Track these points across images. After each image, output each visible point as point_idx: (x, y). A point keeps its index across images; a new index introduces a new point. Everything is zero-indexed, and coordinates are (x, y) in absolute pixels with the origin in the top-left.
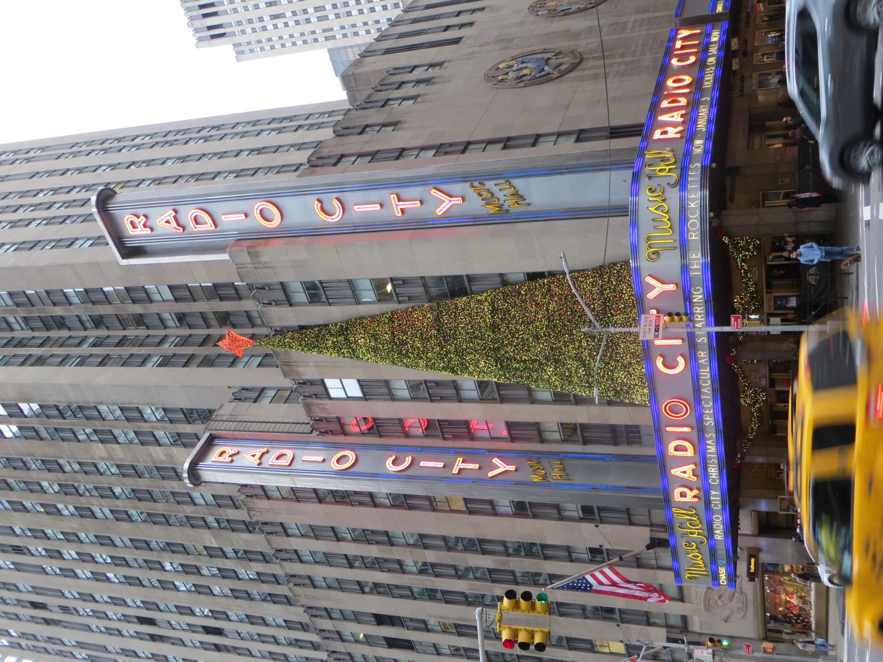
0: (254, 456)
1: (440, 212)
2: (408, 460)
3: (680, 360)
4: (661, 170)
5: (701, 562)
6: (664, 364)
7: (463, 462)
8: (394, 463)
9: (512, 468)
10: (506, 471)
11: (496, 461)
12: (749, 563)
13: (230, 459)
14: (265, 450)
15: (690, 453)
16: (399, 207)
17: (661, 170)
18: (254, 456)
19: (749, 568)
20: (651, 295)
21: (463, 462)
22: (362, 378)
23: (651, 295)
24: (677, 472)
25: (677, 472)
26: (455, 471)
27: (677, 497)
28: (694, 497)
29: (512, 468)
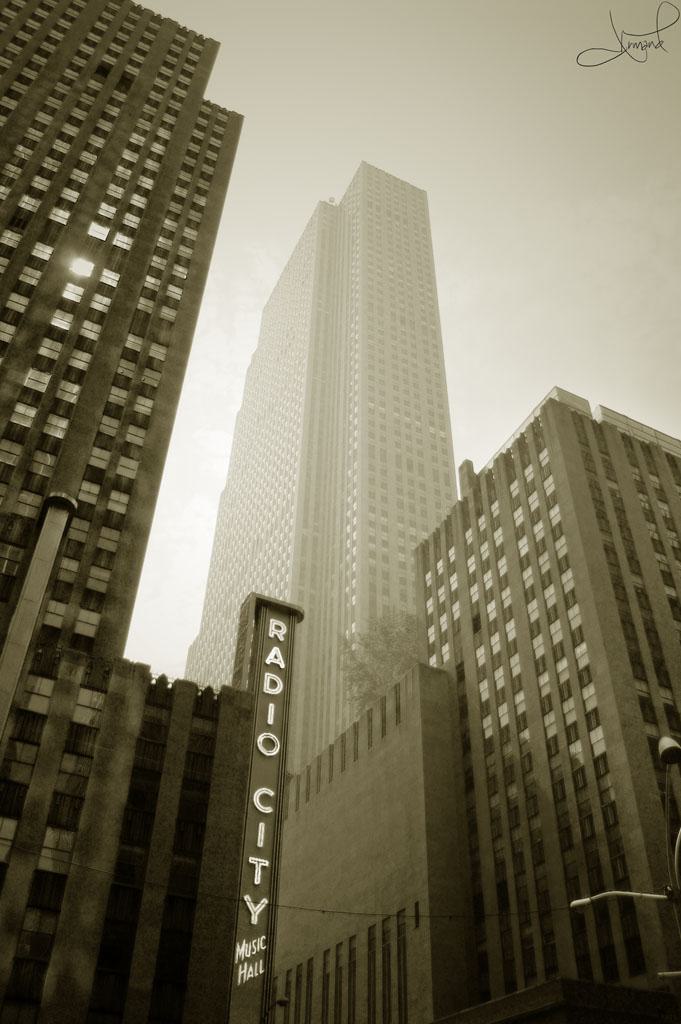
2: (268, 810)
7: (263, 868)
8: (264, 799)
9: (255, 920)
13: (271, 635)
14: (283, 666)
18: (276, 657)
21: (263, 868)
26: (252, 860)
29: (255, 920)
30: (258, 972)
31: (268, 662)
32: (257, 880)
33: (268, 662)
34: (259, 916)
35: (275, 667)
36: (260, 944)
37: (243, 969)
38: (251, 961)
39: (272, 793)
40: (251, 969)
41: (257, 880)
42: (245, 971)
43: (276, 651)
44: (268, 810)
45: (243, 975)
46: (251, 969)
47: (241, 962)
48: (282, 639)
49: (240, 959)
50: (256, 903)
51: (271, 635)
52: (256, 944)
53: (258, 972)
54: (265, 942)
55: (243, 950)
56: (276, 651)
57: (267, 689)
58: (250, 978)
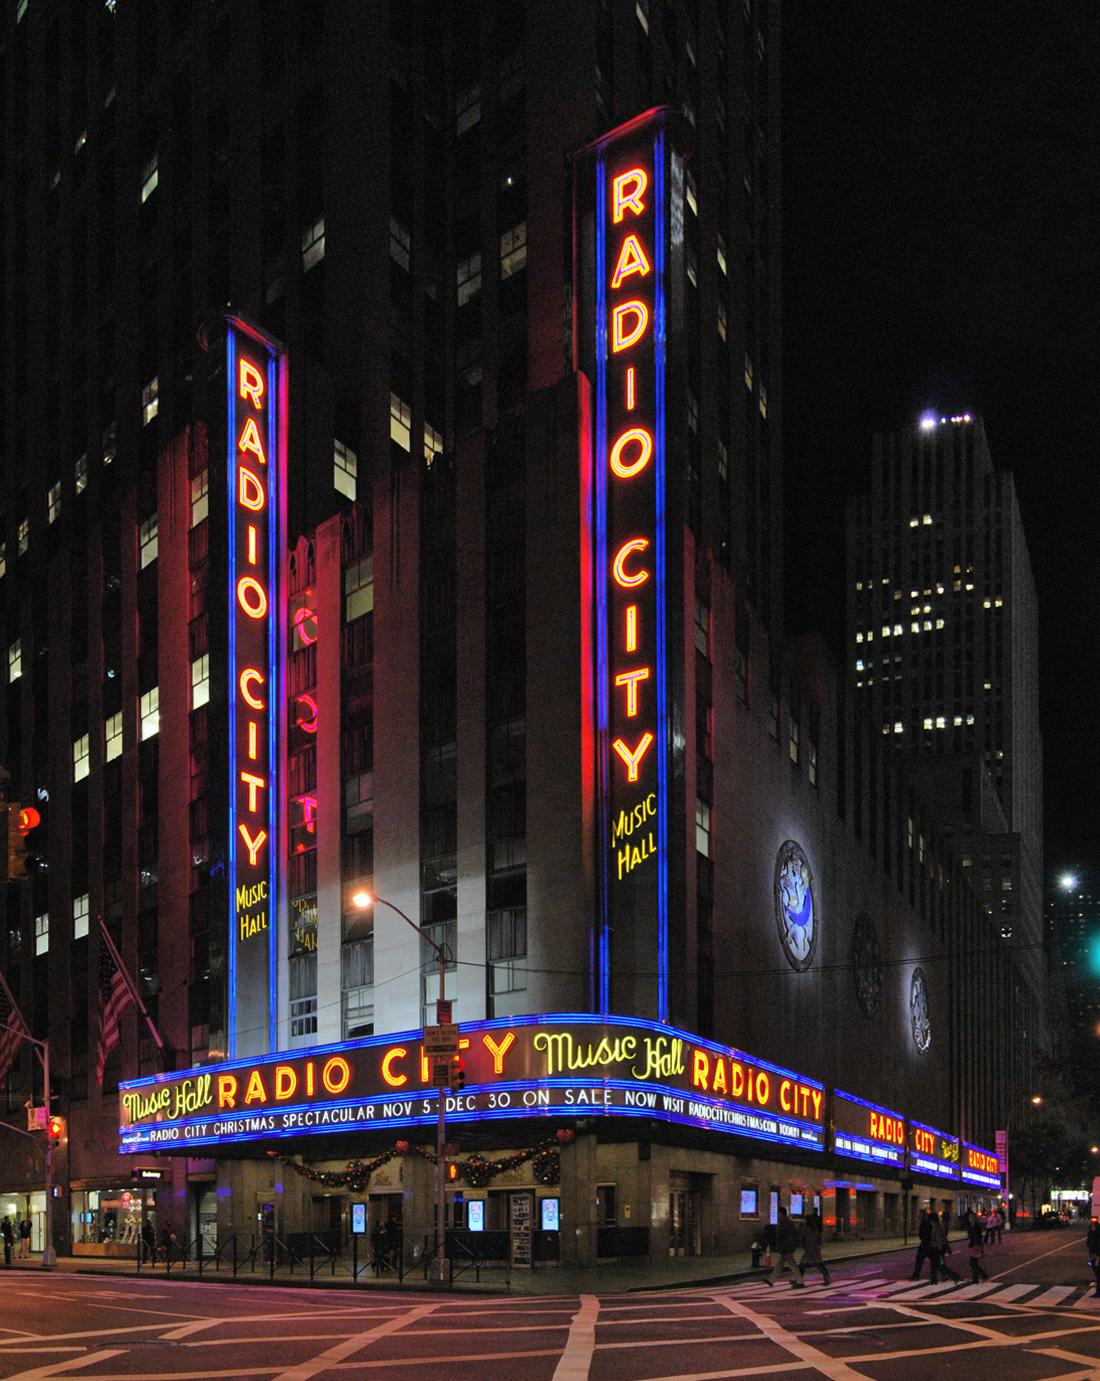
1: (620, 747)
5: (147, 1112)
9: (253, 860)
16: (629, 682)
22: (376, 621)
27: (222, 1081)
29: (253, 860)
30: (261, 927)
36: (259, 893)
37: (245, 922)
38: (252, 912)
40: (253, 921)
42: (247, 924)
45: (245, 928)
46: (253, 921)
47: (244, 912)
49: (241, 907)
52: (256, 890)
53: (261, 927)
54: (266, 890)
55: (242, 898)
58: (253, 933)
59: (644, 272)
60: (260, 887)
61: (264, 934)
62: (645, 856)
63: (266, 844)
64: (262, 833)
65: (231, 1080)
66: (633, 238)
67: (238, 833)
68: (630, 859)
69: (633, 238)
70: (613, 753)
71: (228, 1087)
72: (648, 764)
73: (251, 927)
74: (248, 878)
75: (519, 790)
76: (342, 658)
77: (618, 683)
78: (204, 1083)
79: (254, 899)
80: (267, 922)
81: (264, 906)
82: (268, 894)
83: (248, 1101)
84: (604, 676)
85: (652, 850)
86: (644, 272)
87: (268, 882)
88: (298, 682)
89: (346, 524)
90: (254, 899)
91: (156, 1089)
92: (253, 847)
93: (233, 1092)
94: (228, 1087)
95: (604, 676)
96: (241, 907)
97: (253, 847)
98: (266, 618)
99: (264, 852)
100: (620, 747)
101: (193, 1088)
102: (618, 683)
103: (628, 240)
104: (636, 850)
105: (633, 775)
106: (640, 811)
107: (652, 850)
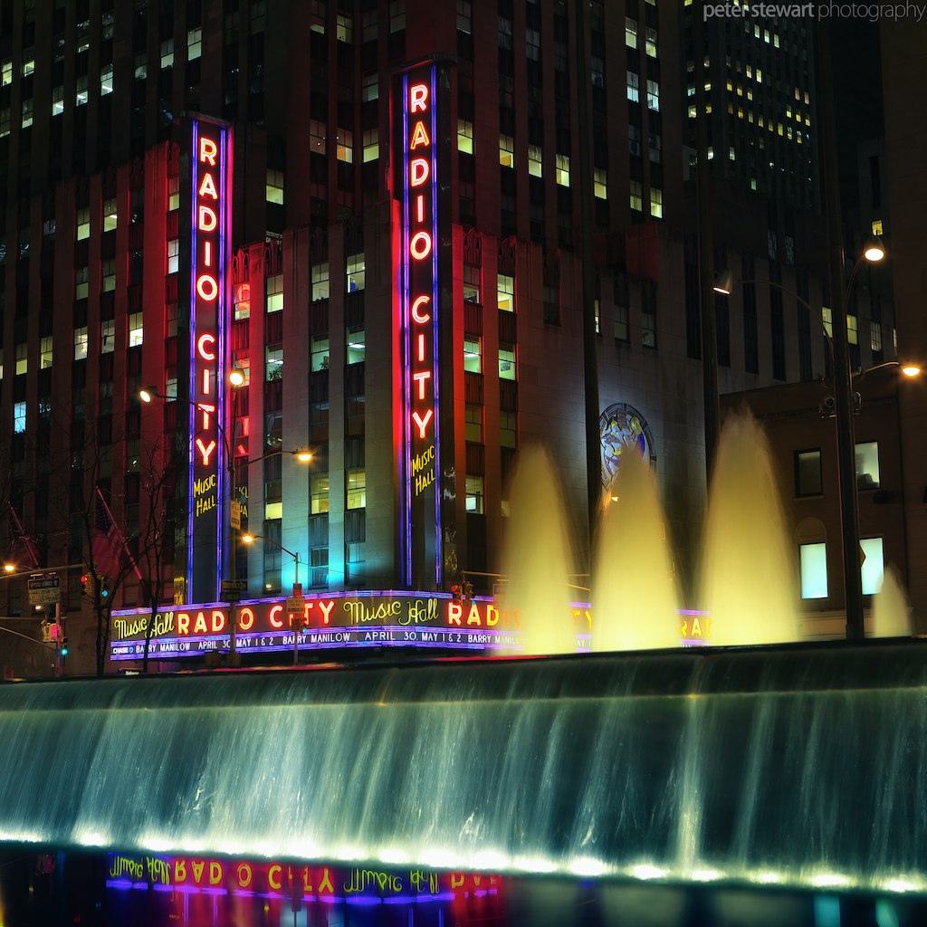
0: (208, 186)
3: (279, 624)
4: (414, 613)
5: (131, 633)
6: (277, 612)
9: (206, 461)
10: (202, 457)
11: (212, 445)
12: (133, 671)
13: (203, 159)
14: (215, 197)
15: (215, 628)
17: (414, 613)
18: (208, 186)
19: (129, 671)
20: (321, 605)
21: (209, 413)
23: (321, 605)
24: (201, 617)
25: (201, 617)
27: (181, 617)
28: (183, 631)
29: (206, 461)
31: (203, 192)
32: (206, 426)
33: (203, 192)
34: (210, 457)
35: (207, 201)
38: (205, 496)
39: (212, 339)
41: (206, 426)
43: (208, 179)
44: (210, 357)
47: (199, 497)
48: (213, 163)
49: (197, 493)
50: (206, 446)
51: (414, 110)
54: (215, 480)
55: (198, 488)
56: (208, 179)
57: (203, 227)
59: (426, 144)
60: (211, 479)
61: (214, 510)
62: (429, 483)
63: (215, 449)
64: (213, 442)
65: (186, 617)
66: (421, 123)
67: (196, 447)
68: (422, 484)
69: (421, 123)
70: (413, 421)
71: (184, 621)
72: (429, 428)
73: (205, 506)
74: (202, 473)
75: (361, 438)
76: (265, 337)
77: (415, 379)
78: (169, 617)
79: (206, 488)
80: (216, 502)
81: (213, 491)
82: (217, 482)
83: (196, 631)
84: (408, 373)
85: (433, 479)
86: (426, 144)
87: (217, 475)
88: (237, 343)
89: (267, 251)
90: (206, 488)
91: (138, 617)
92: (206, 453)
93: (187, 624)
94: (184, 621)
95: (408, 373)
96: (197, 493)
97: (206, 453)
98: (217, 299)
99: (213, 456)
100: (416, 416)
101: (163, 618)
102: (415, 379)
103: (418, 123)
104: (424, 478)
105: (422, 434)
106: (426, 455)
107: (433, 479)
